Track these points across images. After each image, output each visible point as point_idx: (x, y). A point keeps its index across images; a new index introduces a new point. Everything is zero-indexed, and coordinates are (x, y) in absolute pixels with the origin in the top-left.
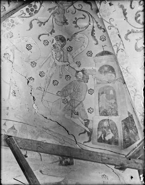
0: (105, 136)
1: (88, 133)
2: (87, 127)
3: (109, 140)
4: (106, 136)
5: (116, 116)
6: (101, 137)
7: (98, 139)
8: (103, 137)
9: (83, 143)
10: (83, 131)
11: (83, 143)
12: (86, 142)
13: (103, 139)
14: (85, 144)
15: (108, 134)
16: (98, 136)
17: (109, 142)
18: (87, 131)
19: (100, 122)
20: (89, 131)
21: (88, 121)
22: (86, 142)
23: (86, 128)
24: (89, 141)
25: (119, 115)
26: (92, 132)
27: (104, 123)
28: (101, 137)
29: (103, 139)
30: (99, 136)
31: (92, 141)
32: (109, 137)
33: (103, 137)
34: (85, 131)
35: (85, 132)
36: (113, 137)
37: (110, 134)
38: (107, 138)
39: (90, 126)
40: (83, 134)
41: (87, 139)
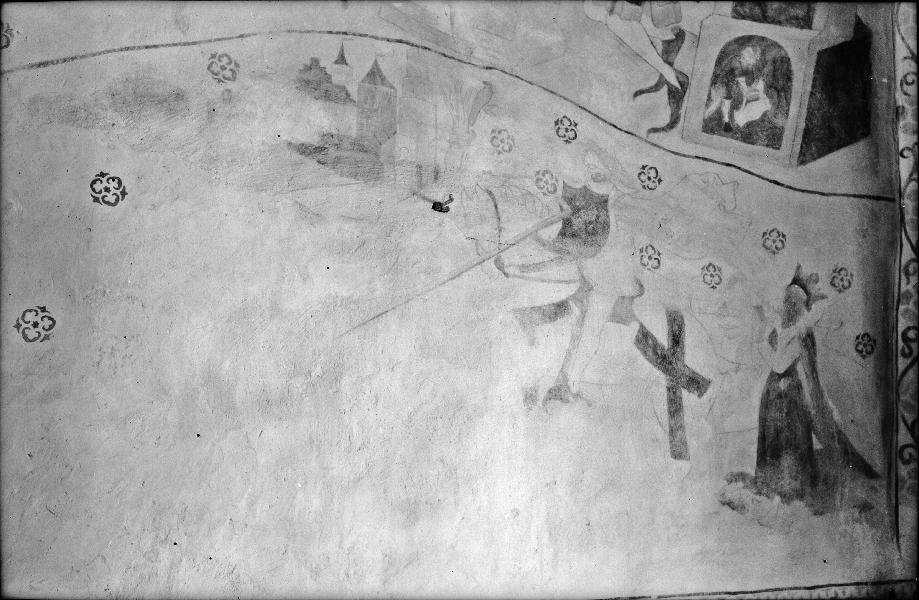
0: (735, 106)
2: (671, 64)
3: (749, 125)
5: (802, 28)
6: (719, 112)
7: (704, 120)
8: (726, 110)
9: (644, 136)
10: (652, 83)
11: (644, 136)
12: (655, 130)
14: (655, 137)
15: (748, 102)
16: (707, 106)
17: (748, 135)
18: (668, 83)
19: (729, 44)
20: (677, 85)
21: (680, 35)
22: (655, 130)
23: (667, 66)
24: (672, 124)
25: (813, 27)
26: (684, 85)
28: (719, 112)
30: (713, 107)
31: (680, 125)
32: (756, 107)
33: (726, 110)
34: (662, 81)
35: (656, 88)
36: (765, 114)
37: (757, 99)
38: (741, 118)
39: (682, 60)
40: (653, 94)
41: (664, 118)
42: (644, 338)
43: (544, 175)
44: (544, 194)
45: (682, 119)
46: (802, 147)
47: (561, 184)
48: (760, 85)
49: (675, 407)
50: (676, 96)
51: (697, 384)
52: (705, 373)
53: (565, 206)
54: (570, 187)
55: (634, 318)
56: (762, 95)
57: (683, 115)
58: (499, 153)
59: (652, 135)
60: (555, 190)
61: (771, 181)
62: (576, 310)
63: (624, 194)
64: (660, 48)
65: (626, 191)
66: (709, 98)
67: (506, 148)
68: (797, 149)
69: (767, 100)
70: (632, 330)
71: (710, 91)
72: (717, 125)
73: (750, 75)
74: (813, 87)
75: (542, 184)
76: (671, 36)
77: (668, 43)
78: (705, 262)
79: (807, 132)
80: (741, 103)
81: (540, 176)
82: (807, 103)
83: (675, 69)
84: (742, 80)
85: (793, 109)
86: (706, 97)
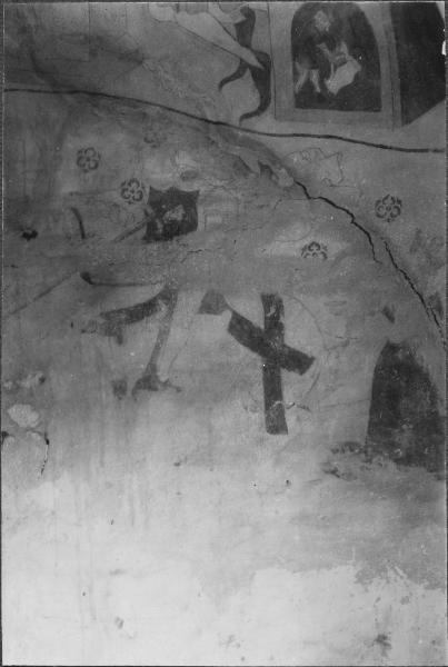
0: (325, 75)
1: (254, 69)
2: (248, 46)
3: (343, 90)
4: (328, 77)
6: (308, 84)
7: (296, 95)
9: (237, 124)
10: (234, 69)
12: (247, 116)
13: (318, 90)
15: (336, 68)
16: (295, 80)
27: (316, 17)
28: (308, 84)
29: (318, 90)
30: (302, 80)
32: (344, 76)
34: (244, 66)
36: (357, 77)
37: (345, 63)
38: (334, 84)
39: (259, 38)
41: (252, 100)
42: (239, 326)
43: (129, 184)
44: (130, 203)
45: (272, 100)
46: (402, 104)
47: (148, 190)
48: (344, 48)
49: (273, 391)
50: (262, 76)
51: (300, 362)
52: (308, 350)
53: (150, 211)
54: (157, 192)
55: (226, 306)
56: (348, 57)
57: (273, 94)
58: (86, 171)
59: (245, 121)
60: (141, 197)
61: (377, 146)
62: (164, 309)
63: (216, 187)
64: (234, 32)
65: (218, 183)
66: (296, 73)
67: (92, 165)
68: (398, 107)
69: (355, 62)
70: (224, 319)
71: (294, 65)
72: (310, 99)
73: (330, 40)
74: (396, 38)
75: (126, 194)
76: (241, 18)
77: (239, 26)
78: (307, 242)
79: (404, 88)
80: (330, 70)
81: (126, 186)
82: (395, 56)
83: (252, 50)
84: (323, 46)
85: (384, 65)
86: (291, 71)
